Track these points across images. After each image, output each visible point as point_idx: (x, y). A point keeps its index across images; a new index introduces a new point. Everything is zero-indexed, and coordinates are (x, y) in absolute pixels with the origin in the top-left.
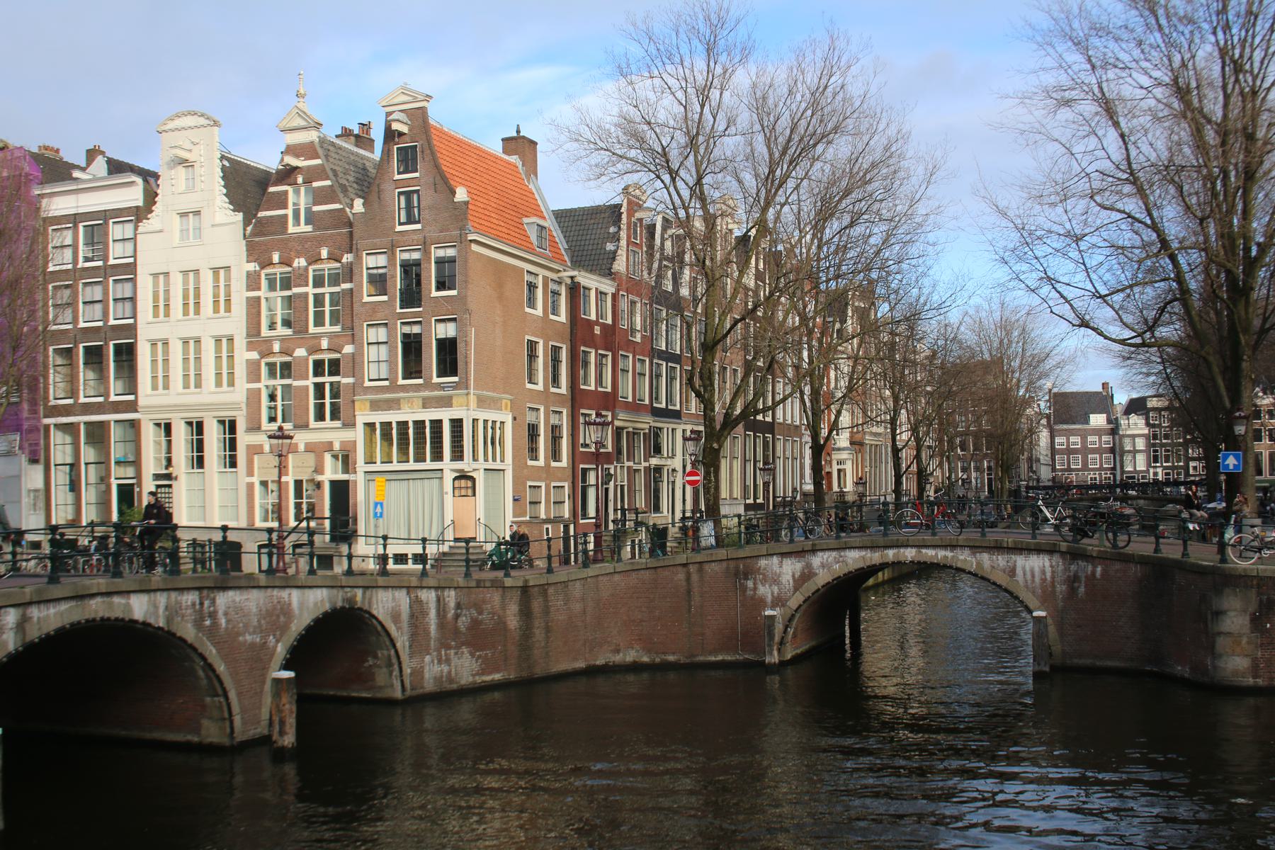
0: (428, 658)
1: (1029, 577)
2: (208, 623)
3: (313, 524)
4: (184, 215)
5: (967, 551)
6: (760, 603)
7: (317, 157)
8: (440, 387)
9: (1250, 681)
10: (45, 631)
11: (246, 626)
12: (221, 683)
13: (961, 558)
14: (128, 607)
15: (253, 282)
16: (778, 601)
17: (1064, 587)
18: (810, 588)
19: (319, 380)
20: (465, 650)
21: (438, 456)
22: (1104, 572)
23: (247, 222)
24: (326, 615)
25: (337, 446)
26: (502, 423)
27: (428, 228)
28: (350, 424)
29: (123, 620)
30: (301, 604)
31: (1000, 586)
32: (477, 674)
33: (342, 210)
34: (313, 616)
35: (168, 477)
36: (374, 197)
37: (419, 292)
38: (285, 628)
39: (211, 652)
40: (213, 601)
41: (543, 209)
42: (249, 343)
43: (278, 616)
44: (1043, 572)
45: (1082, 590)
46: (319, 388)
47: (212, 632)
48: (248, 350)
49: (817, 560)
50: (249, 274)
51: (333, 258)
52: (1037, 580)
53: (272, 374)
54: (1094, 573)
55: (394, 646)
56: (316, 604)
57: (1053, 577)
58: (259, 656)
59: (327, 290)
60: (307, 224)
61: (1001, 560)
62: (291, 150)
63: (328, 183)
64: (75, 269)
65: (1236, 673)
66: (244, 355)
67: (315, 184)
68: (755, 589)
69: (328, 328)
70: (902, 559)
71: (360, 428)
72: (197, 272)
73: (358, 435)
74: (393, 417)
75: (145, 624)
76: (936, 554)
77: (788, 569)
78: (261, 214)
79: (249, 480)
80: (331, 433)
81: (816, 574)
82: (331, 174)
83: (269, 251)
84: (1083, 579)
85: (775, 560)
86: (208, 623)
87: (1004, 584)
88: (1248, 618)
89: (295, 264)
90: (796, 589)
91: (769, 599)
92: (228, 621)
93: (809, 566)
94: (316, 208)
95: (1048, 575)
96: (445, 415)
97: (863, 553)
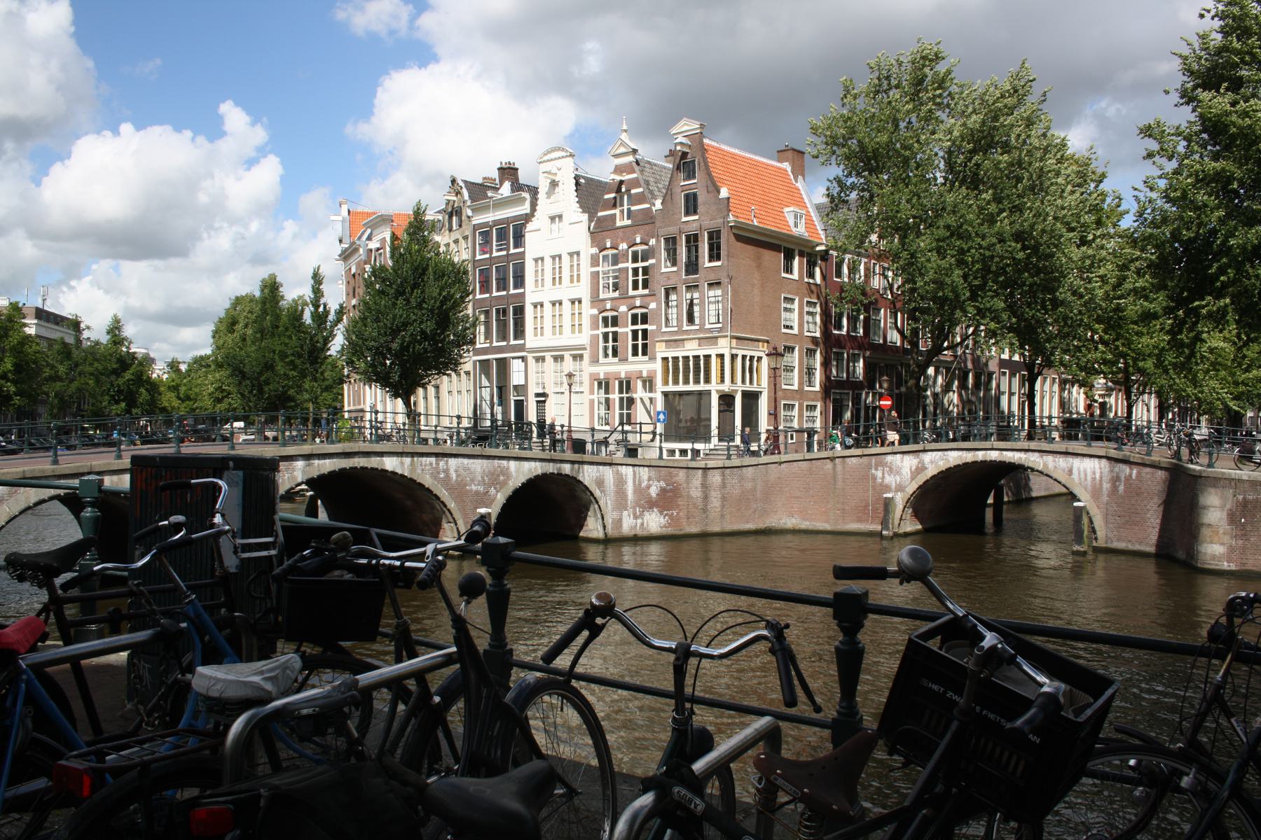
0: (625, 513)
1: (1082, 476)
2: (442, 476)
3: (627, 428)
4: (553, 219)
5: (1037, 454)
6: (887, 488)
7: (634, 172)
8: (710, 330)
9: (1225, 566)
10: (322, 472)
11: (472, 480)
12: (451, 514)
13: (1032, 459)
14: (383, 463)
15: (595, 261)
16: (900, 488)
17: (1109, 485)
18: (921, 479)
19: (635, 327)
20: (655, 510)
21: (707, 380)
22: (1139, 474)
23: (590, 221)
24: (537, 477)
25: (645, 374)
26: (760, 359)
27: (703, 218)
28: (653, 359)
29: (377, 469)
30: (517, 471)
31: (1059, 482)
32: (665, 526)
33: (649, 209)
34: (527, 478)
35: (544, 395)
36: (668, 197)
37: (697, 265)
38: (504, 483)
39: (443, 494)
40: (447, 463)
41: (806, 201)
42: (592, 302)
43: (498, 476)
44: (1094, 473)
45: (1121, 488)
46: (635, 333)
47: (446, 482)
48: (592, 307)
49: (927, 457)
50: (592, 255)
51: (644, 243)
52: (1089, 478)
53: (606, 326)
54: (1130, 475)
55: (597, 502)
56: (530, 470)
57: (1101, 477)
58: (484, 499)
59: (640, 264)
60: (628, 218)
61: (1062, 462)
62: (618, 170)
63: (640, 190)
64: (491, 258)
65: (1214, 557)
66: (588, 311)
67: (633, 191)
68: (883, 478)
69: (641, 291)
70: (988, 459)
71: (659, 361)
72: (560, 257)
73: (658, 366)
74: (680, 354)
75: (394, 473)
76: (985, 455)
77: (907, 464)
78: (600, 214)
79: (592, 397)
80: (640, 365)
81: (926, 468)
82: (642, 183)
83: (604, 240)
84: (1123, 479)
85: (898, 456)
86: (442, 476)
87: (1063, 481)
88: (1225, 513)
89: (620, 248)
90: (912, 479)
91: (893, 486)
92: (458, 476)
93: (921, 462)
94: (633, 208)
95: (1098, 476)
96: (713, 352)
97: (960, 453)
